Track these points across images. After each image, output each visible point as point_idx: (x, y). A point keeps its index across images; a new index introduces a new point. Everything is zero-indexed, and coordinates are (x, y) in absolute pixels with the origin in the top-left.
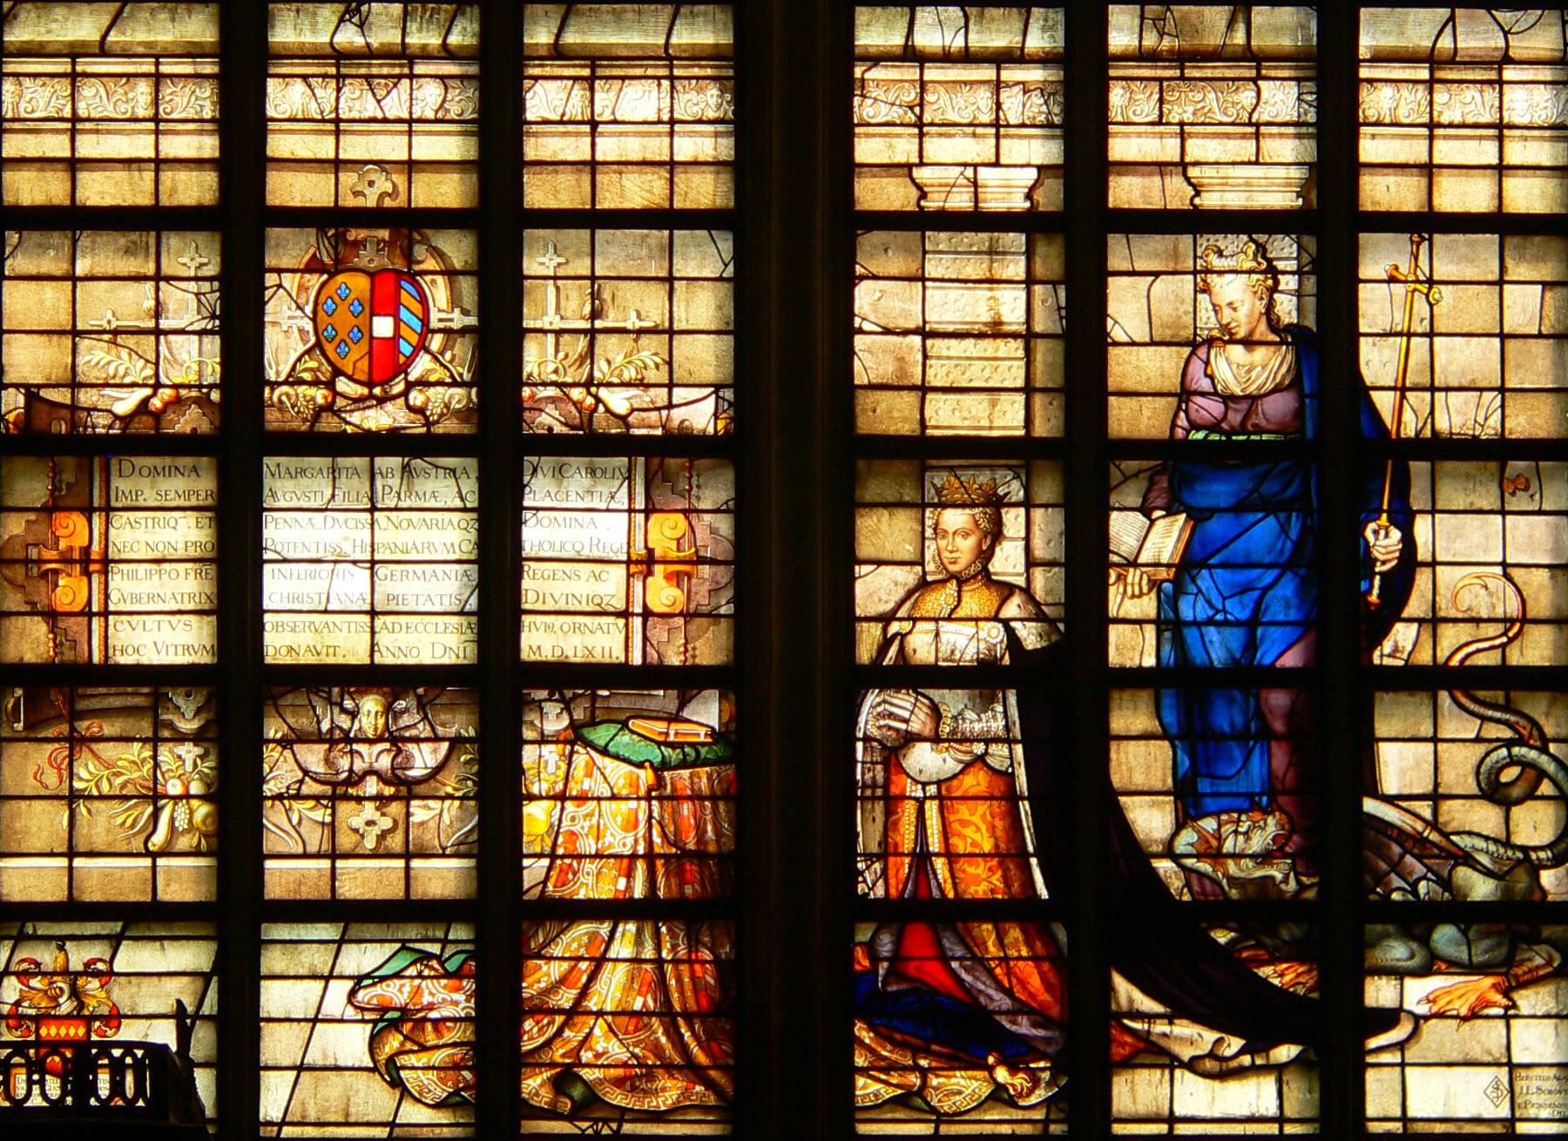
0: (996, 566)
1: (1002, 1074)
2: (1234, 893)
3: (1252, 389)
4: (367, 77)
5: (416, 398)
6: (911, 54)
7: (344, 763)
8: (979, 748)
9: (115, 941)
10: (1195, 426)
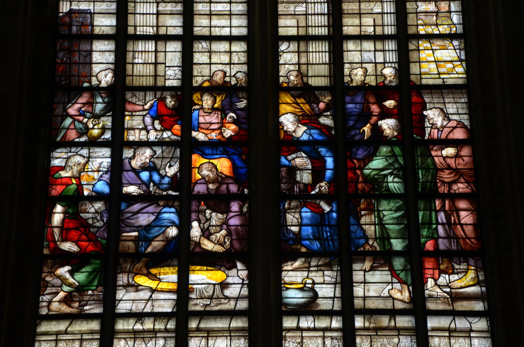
4: (143, 338)
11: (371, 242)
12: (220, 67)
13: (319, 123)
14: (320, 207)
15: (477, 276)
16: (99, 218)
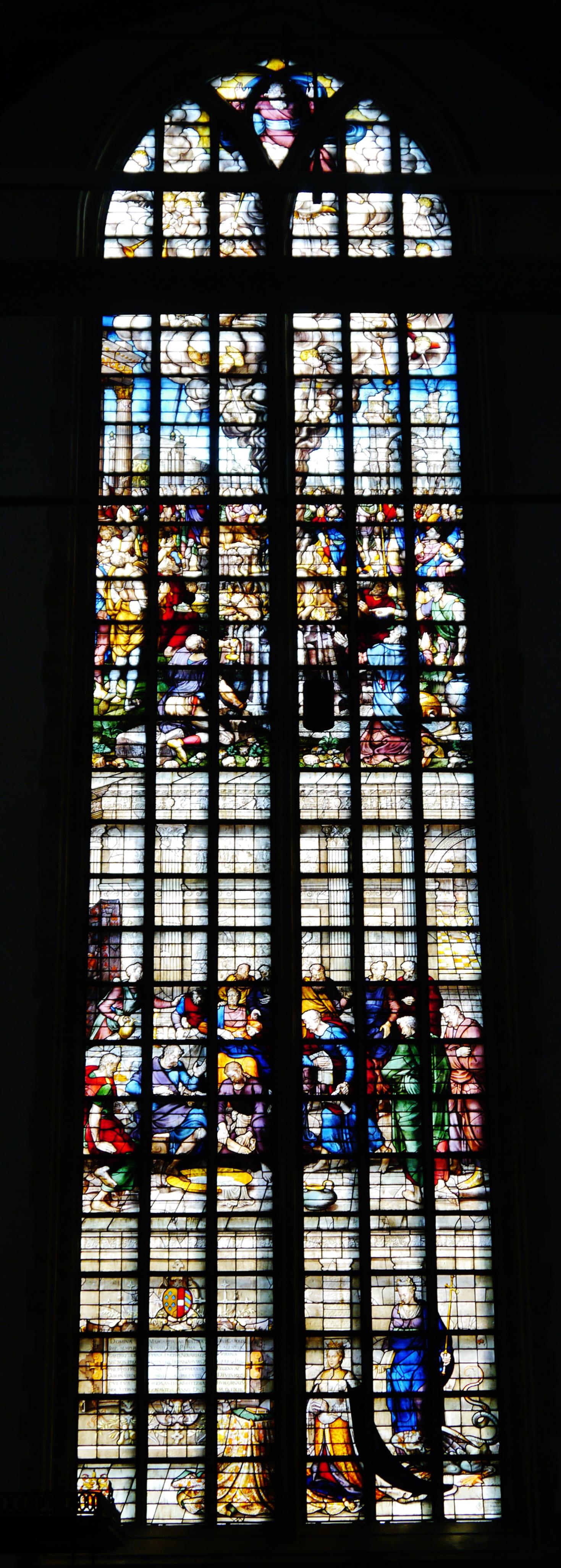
0: (342, 1365)
1: (347, 1504)
2: (408, 1453)
3: (410, 1317)
5: (189, 1321)
6: (319, 1229)
7: (170, 1420)
8: (339, 1414)
9: (109, 1469)
10: (395, 1327)
11: (387, 1144)
12: (245, 960)
13: (340, 1020)
14: (340, 1109)
15: (483, 1177)
16: (132, 1119)
